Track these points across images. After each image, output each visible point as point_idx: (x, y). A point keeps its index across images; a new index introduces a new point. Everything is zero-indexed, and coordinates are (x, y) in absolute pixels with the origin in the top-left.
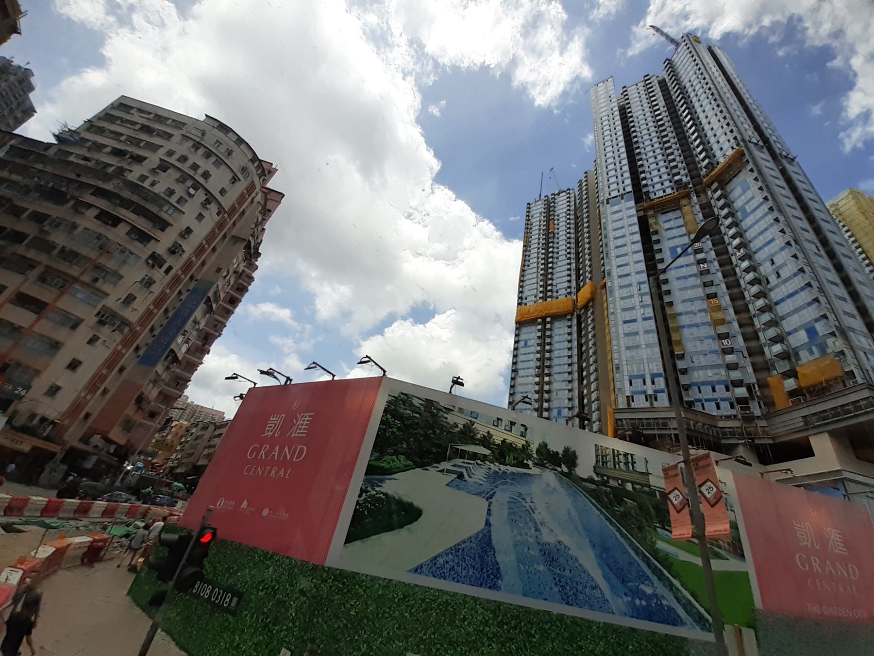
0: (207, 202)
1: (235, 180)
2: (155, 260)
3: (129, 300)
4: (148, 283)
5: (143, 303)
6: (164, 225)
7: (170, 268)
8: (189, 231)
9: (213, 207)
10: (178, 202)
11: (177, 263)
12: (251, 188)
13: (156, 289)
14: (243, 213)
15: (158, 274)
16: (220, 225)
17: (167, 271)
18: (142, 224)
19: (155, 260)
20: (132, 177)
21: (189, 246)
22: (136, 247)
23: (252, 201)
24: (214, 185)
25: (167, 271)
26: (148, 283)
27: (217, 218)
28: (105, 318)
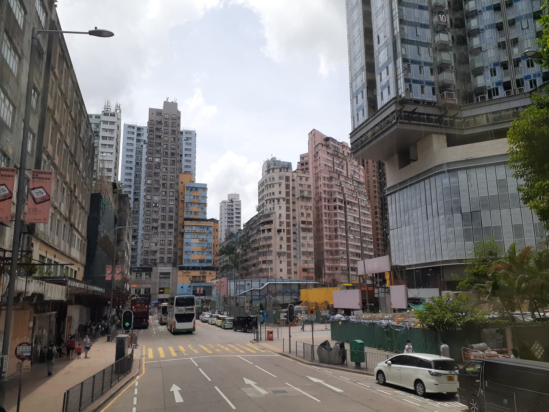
0: (279, 200)
1: (280, 185)
2: (279, 231)
3: (281, 246)
4: (282, 238)
5: (284, 245)
6: (271, 222)
7: (284, 230)
8: (280, 215)
9: (281, 200)
10: (273, 210)
11: (284, 227)
12: (287, 179)
13: (285, 239)
14: (294, 188)
15: (282, 234)
16: (288, 202)
17: (284, 232)
18: (267, 227)
19: (279, 231)
20: (265, 213)
21: (284, 219)
22: (270, 234)
23: (293, 180)
24: (277, 195)
25: (284, 232)
26: (282, 238)
27: (285, 202)
28: (280, 254)
